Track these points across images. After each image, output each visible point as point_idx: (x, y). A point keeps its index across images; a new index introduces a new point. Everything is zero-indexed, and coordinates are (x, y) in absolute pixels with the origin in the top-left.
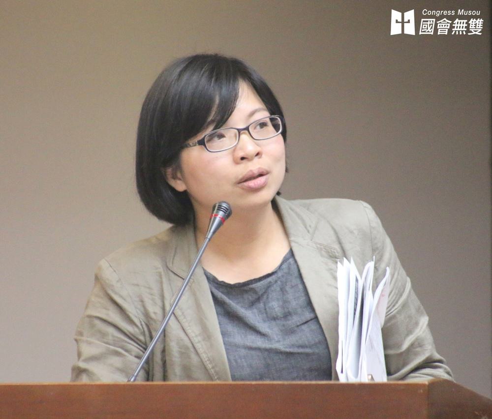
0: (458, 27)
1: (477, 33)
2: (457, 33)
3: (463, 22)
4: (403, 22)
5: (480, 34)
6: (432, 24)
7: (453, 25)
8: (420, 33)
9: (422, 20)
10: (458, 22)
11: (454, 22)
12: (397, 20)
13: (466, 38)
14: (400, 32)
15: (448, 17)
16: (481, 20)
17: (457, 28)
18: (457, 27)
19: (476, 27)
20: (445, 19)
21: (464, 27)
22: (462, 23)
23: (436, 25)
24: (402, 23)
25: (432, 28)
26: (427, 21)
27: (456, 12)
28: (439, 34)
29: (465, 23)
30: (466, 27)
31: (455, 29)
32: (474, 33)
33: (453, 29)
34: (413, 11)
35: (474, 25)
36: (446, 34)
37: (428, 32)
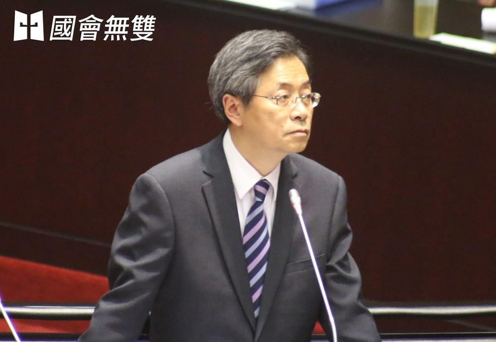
0: (115, 29)
1: (145, 38)
2: (112, 39)
3: (123, 22)
5: (151, 40)
6: (71, 24)
7: (106, 26)
8: (52, 38)
9: (55, 17)
10: (114, 21)
11: (108, 21)
13: (127, 47)
16: (153, 18)
17: (112, 30)
18: (112, 28)
19: (143, 28)
20: (92, 16)
21: (124, 29)
22: (120, 22)
23: (78, 25)
25: (70, 30)
26: (63, 20)
28: (82, 39)
29: (125, 22)
30: (127, 29)
31: (110, 32)
32: (141, 38)
33: (106, 32)
35: (139, 26)
36: (94, 39)
37: (65, 36)
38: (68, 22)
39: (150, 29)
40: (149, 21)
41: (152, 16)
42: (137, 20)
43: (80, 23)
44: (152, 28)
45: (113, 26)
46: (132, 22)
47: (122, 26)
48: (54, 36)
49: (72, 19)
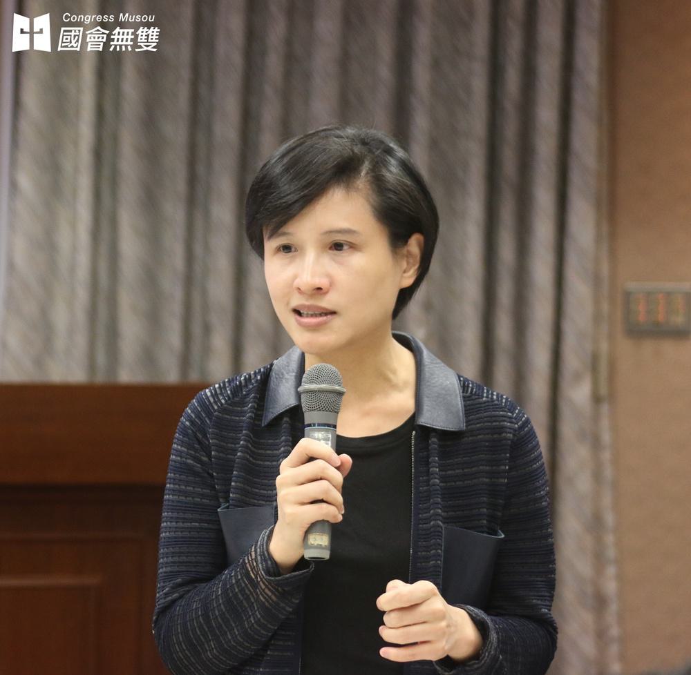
0: (120, 40)
1: (149, 49)
2: (118, 49)
3: (128, 33)
4: (31, 33)
5: (155, 50)
6: (79, 36)
7: (112, 37)
8: (60, 49)
9: (63, 29)
10: (119, 33)
11: (113, 33)
12: (22, 31)
14: (27, 47)
15: (103, 25)
16: (157, 29)
17: (118, 41)
18: (118, 39)
19: (148, 39)
21: (129, 40)
24: (31, 34)
25: (77, 41)
26: (71, 31)
27: (117, 18)
28: (89, 49)
29: (130, 33)
30: (132, 40)
31: (115, 43)
32: (145, 48)
33: (112, 43)
34: (48, 15)
35: (144, 37)
36: (101, 49)
37: (72, 47)
38: (76, 34)
39: (154, 40)
40: (153, 32)
41: (156, 28)
42: (142, 31)
43: (87, 35)
44: (156, 39)
45: (118, 37)
46: (137, 33)
47: (127, 37)
48: (62, 47)
49: (79, 31)
